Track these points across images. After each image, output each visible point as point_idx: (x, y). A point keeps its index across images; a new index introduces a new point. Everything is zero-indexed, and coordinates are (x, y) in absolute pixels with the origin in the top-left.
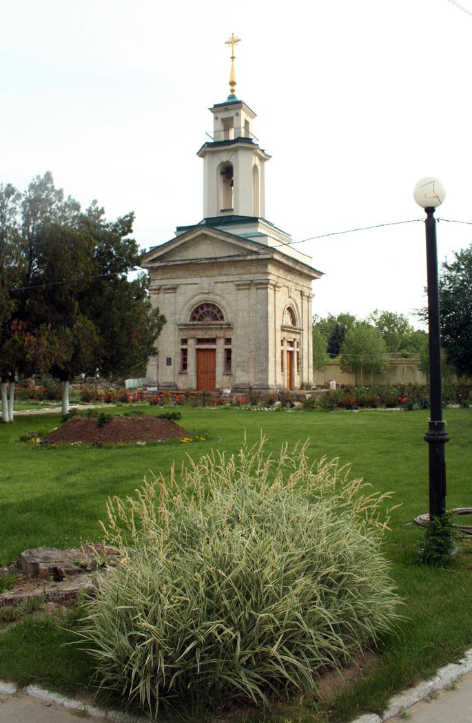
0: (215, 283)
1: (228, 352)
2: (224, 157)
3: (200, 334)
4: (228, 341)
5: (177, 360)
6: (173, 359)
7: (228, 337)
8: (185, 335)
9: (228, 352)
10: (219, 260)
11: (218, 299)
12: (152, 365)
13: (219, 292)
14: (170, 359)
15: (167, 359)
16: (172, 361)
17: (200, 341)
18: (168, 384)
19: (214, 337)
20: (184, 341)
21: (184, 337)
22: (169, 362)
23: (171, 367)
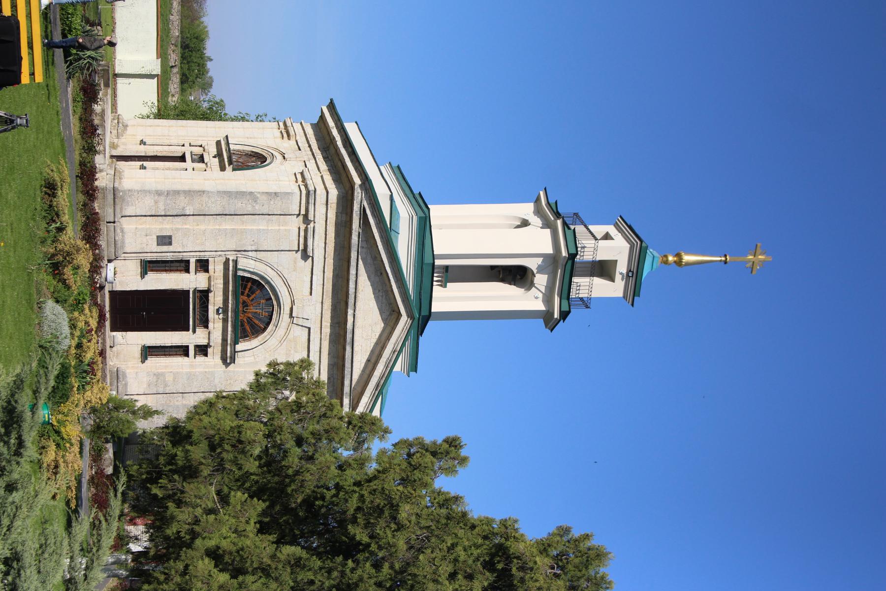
0: (309, 329)
1: (183, 351)
2: (541, 280)
3: (216, 300)
4: (202, 350)
5: (166, 253)
6: (171, 248)
7: (210, 350)
8: (216, 269)
9: (183, 351)
10: (348, 348)
11: (281, 331)
12: (156, 202)
13: (291, 336)
14: (170, 244)
15: (170, 237)
16: (165, 248)
17: (204, 295)
18: (119, 244)
19: (211, 325)
20: (203, 265)
21: (211, 267)
22: (164, 240)
23: (154, 247)
